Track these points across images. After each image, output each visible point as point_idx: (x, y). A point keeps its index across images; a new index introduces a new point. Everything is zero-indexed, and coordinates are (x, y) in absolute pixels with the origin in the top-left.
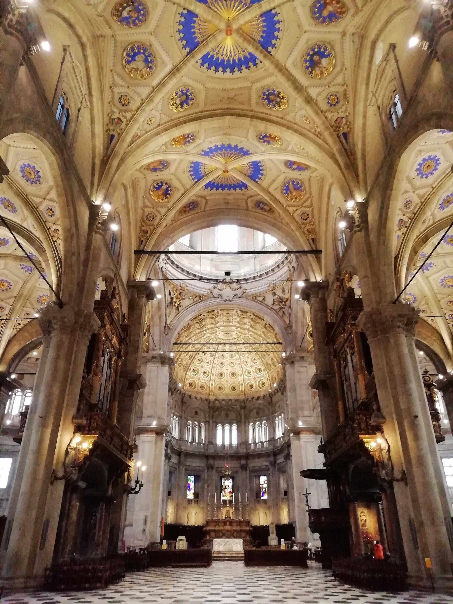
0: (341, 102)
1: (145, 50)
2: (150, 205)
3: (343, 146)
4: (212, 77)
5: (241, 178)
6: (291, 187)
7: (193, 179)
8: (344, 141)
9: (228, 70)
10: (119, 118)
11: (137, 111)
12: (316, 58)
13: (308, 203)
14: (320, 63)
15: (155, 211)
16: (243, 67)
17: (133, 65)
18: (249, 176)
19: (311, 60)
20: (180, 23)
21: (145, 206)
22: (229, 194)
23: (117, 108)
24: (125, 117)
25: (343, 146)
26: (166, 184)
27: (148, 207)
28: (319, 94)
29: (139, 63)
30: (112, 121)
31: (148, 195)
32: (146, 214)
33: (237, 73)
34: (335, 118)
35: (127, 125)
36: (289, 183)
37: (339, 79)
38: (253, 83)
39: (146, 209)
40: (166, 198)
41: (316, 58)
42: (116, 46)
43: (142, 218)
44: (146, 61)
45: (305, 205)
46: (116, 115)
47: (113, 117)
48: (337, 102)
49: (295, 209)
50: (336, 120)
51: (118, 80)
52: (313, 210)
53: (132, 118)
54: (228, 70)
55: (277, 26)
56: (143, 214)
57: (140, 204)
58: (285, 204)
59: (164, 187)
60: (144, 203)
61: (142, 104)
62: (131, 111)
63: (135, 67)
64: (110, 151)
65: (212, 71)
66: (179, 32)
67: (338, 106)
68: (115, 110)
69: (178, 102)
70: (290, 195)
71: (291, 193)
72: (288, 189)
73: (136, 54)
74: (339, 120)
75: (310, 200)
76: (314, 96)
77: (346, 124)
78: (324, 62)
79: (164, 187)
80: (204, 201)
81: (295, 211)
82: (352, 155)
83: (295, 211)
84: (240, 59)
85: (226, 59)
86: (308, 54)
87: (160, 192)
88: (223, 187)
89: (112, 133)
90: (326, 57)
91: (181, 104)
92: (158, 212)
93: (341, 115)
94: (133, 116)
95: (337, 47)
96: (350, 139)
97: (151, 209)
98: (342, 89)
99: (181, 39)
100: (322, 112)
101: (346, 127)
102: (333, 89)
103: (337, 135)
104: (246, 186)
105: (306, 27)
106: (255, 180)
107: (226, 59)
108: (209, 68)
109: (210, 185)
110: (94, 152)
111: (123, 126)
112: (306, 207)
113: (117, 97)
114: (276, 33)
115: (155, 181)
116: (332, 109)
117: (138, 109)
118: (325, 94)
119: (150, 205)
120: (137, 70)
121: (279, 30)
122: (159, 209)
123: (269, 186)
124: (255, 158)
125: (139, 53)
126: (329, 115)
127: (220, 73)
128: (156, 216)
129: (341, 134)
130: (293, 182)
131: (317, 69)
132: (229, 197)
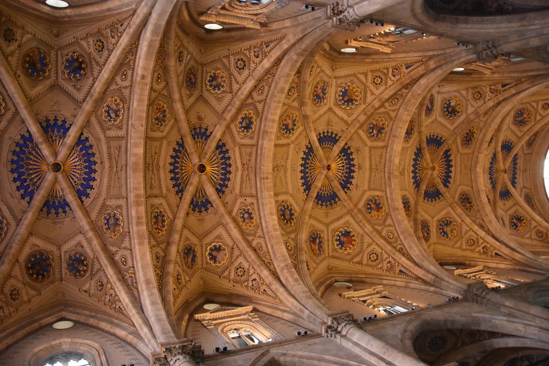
0: (479, 90)
1: (441, 225)
2: (529, 234)
3: (513, 86)
5: (510, 159)
6: (520, 119)
7: (509, 197)
8: (508, 86)
10: (483, 248)
11: (478, 235)
12: (450, 109)
13: (535, 105)
14: (453, 106)
15: (535, 230)
17: (449, 233)
18: (509, 153)
19: (450, 113)
21: (530, 238)
22: (520, 169)
23: (476, 248)
24: (482, 243)
25: (513, 86)
26: (513, 219)
27: (531, 235)
28: (472, 106)
29: (448, 229)
30: (485, 253)
31: (521, 234)
32: (536, 237)
33: (453, 163)
34: (490, 94)
35: (488, 243)
36: (516, 121)
37: (464, 93)
38: (458, 151)
39: (533, 237)
40: (523, 220)
41: (450, 109)
42: (439, 244)
43: (540, 241)
44: (447, 225)
45: (536, 107)
46: (480, 248)
47: (482, 252)
48: (479, 93)
49: (538, 115)
50: (492, 93)
51: (458, 245)
52: (541, 100)
53: (483, 239)
56: (537, 240)
57: (528, 241)
58: (533, 123)
59: (515, 221)
60: (528, 238)
61: (473, 231)
62: (478, 239)
63: (450, 232)
64: (508, 257)
65: (451, 180)
66: (432, 201)
67: (482, 92)
68: (477, 250)
69: (468, 205)
70: (526, 119)
71: (524, 118)
72: (520, 121)
73: (443, 231)
74: (492, 91)
75: (532, 103)
76: (473, 109)
77: (495, 86)
78: (452, 104)
79: (515, 221)
80: (524, 190)
81: (540, 115)
82: (521, 80)
83: (540, 115)
85: (445, 170)
86: (448, 115)
87: (519, 225)
88: (515, 173)
89: (494, 255)
90: (450, 103)
91: (470, 203)
92: (535, 227)
93: (488, 89)
94: (481, 238)
95: (445, 96)
96: (507, 82)
97: (533, 233)
98: (471, 90)
100: (484, 103)
101: (498, 86)
102: (470, 97)
103: (503, 91)
104: (516, 155)
106: (512, 148)
107: (445, 170)
109: (513, 183)
110: (510, 269)
111: (488, 245)
112: (538, 106)
113: (468, 247)
115: (510, 228)
116: (483, 96)
117: (476, 234)
118: (473, 102)
119: (529, 234)
120: (452, 232)
122: (533, 226)
123: (517, 136)
124: (499, 149)
125: (442, 229)
126: (488, 98)
127: (452, 175)
128: (539, 230)
129: (503, 89)
130: (516, 117)
131: (457, 108)
132: (522, 169)
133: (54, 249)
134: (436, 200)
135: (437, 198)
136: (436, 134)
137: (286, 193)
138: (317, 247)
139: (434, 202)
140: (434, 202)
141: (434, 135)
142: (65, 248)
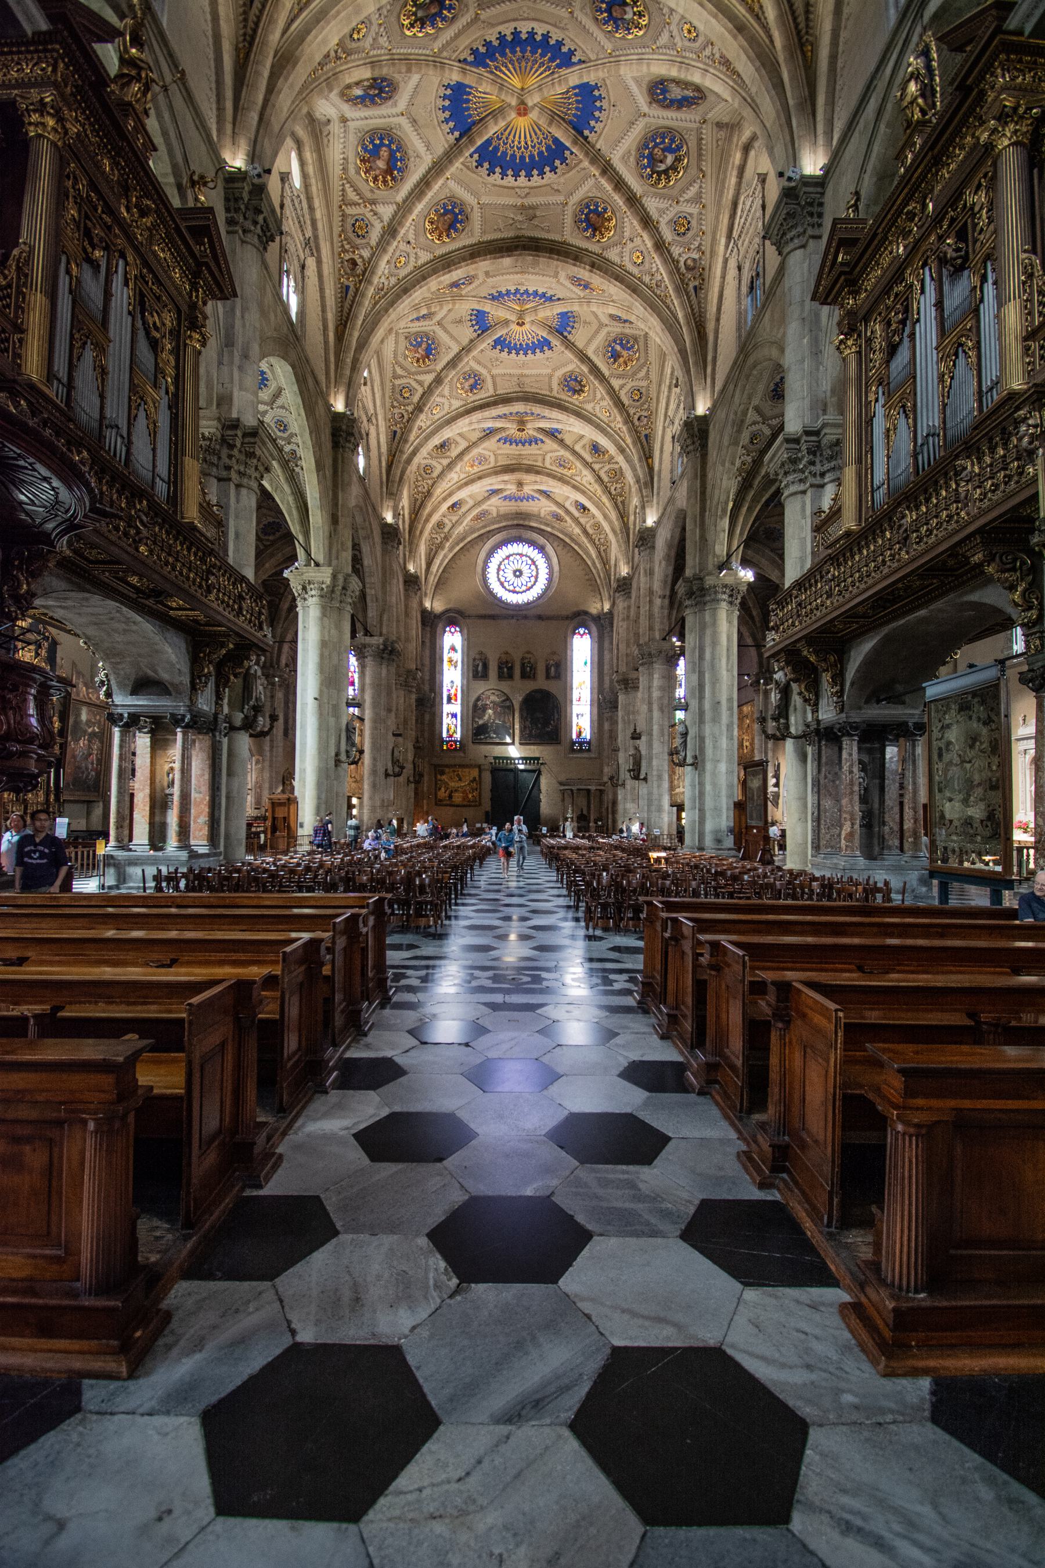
4: (555, 26)
9: (524, 36)
16: (496, 43)
20: (597, 120)
38: (476, 18)
54: (524, 36)
55: (447, 114)
65: (556, 36)
66: (600, 109)
84: (503, 54)
99: (600, 98)
105: (403, 121)
107: (528, 54)
108: (560, 44)
114: (447, 103)
121: (444, 109)
127: (540, 30)
133: (604, 332)
134: (600, 98)
135: (598, 104)
136: (440, 103)
137: (551, 376)
138: (625, 353)
139: (605, 104)
140: (605, 104)
141: (444, 109)
142: (645, 108)
